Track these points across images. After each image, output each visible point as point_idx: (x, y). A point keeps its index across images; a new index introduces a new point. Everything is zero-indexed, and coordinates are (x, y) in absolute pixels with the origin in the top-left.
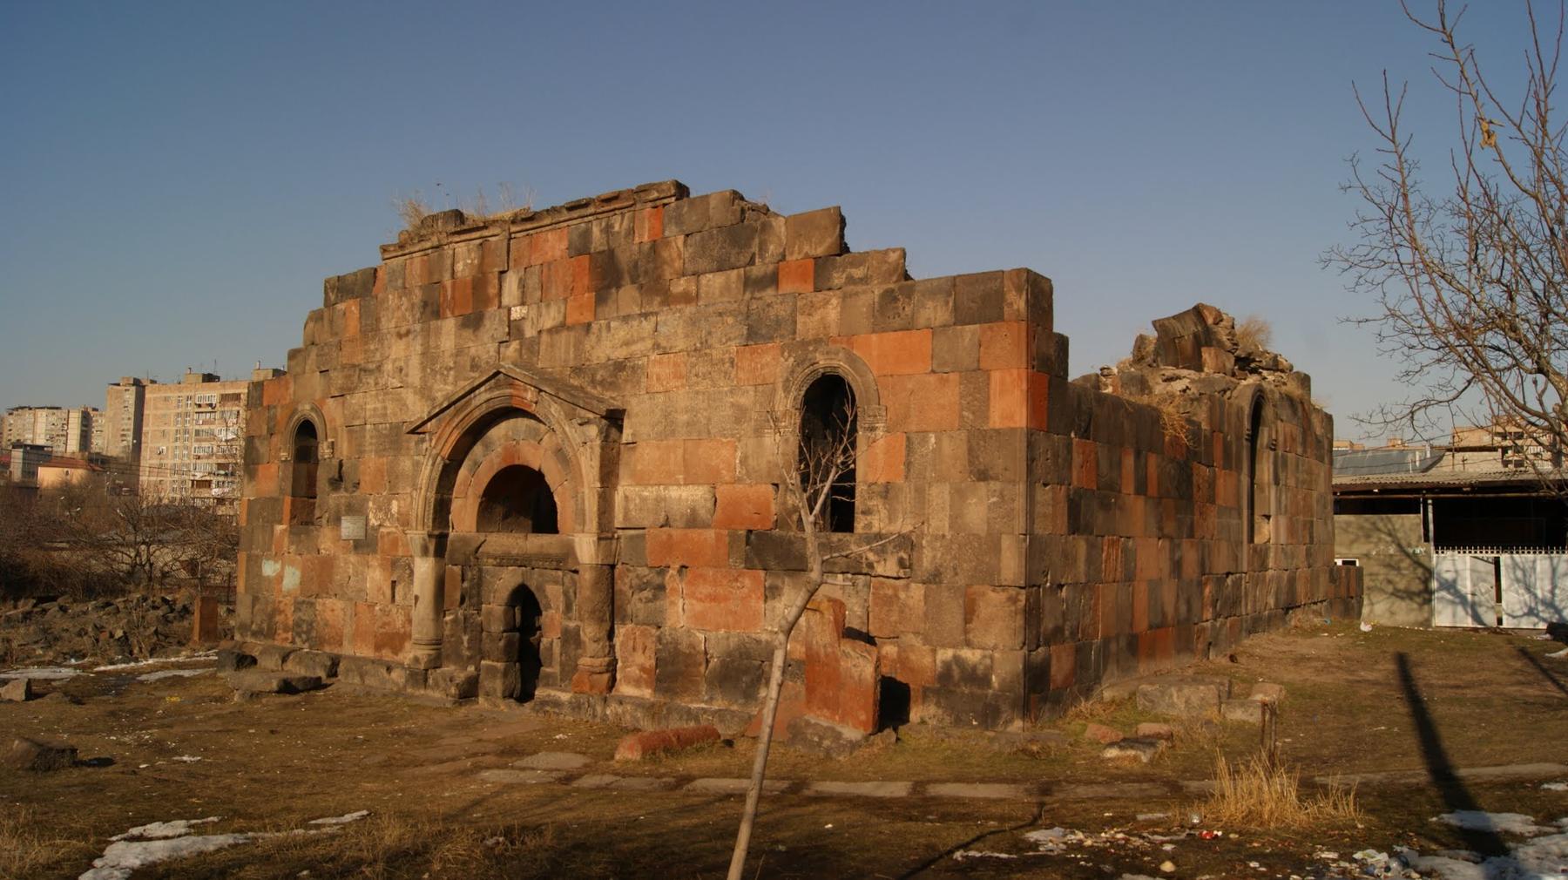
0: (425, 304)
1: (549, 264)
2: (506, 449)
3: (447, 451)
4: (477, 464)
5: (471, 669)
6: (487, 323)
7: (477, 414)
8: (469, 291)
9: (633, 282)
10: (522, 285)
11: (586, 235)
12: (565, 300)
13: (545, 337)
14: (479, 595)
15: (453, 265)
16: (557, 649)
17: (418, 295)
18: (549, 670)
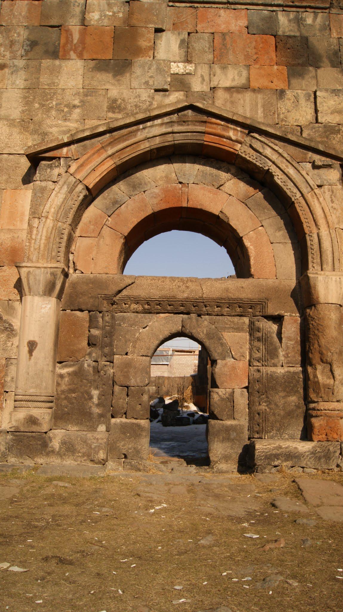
0: (33, 44)
1: (224, 34)
2: (166, 191)
3: (92, 181)
4: (117, 204)
5: (102, 428)
6: (137, 70)
7: (145, 146)
8: (108, 39)
9: (333, 66)
10: (185, 45)
11: (272, 21)
12: (248, 67)
13: (221, 95)
14: (111, 345)
15: (84, 13)
16: (242, 400)
17: (21, 35)
18: (229, 422)
